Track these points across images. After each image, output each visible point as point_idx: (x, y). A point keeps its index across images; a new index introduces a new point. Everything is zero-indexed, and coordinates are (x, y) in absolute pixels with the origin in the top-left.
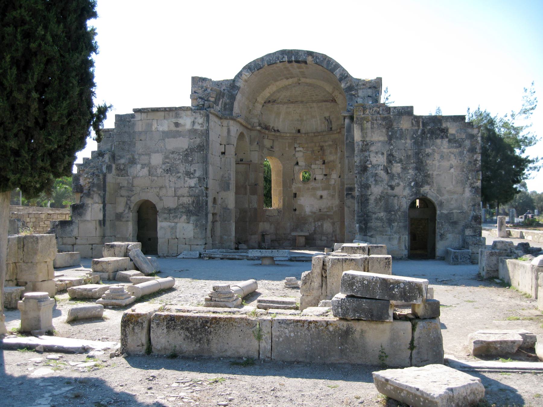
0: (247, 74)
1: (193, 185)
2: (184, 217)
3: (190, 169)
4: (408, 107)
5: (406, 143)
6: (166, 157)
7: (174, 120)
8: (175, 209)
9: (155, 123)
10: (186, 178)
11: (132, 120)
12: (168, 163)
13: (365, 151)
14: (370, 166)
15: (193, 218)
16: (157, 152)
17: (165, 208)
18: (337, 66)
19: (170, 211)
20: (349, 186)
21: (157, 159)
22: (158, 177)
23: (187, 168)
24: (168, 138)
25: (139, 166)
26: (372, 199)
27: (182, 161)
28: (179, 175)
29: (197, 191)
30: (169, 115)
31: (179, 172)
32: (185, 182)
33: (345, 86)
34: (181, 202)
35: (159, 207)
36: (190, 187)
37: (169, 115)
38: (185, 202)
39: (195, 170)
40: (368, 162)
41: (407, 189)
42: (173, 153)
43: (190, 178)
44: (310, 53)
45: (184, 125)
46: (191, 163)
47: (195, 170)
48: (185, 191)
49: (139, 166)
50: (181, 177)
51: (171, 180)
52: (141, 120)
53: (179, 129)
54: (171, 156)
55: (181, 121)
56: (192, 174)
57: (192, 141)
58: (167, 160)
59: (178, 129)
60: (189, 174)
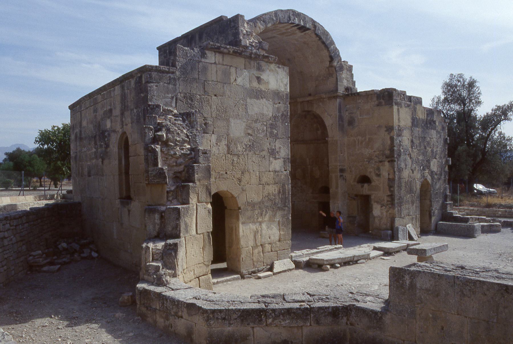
0: (262, 27)
1: (278, 169)
2: (270, 213)
3: (275, 146)
4: (417, 98)
5: (419, 131)
6: (249, 127)
7: (256, 73)
8: (260, 203)
9: (233, 70)
10: (271, 159)
11: (203, 60)
12: (251, 135)
13: (400, 136)
14: (402, 151)
15: (279, 214)
16: (237, 116)
17: (248, 203)
18: (332, 43)
19: (252, 205)
20: (341, 167)
21: (237, 128)
22: (238, 156)
23: (272, 144)
24: (251, 98)
25: (214, 138)
26: (403, 181)
27: (266, 134)
28: (264, 153)
29: (283, 177)
30: (250, 63)
31: (263, 150)
32: (270, 163)
33: (337, 64)
34: (266, 193)
35: (241, 201)
36: (275, 172)
37: (250, 63)
38: (271, 192)
39: (280, 148)
40: (401, 147)
41: (420, 171)
42: (256, 121)
43: (275, 159)
44: (314, 22)
45: (268, 83)
46: (276, 137)
47: (280, 148)
48: (268, 177)
49: (214, 138)
50: (266, 157)
51: (254, 160)
52: (215, 63)
53: (263, 87)
54: (254, 125)
55: (264, 76)
56: (278, 152)
57: (276, 106)
58: (250, 132)
59: (261, 87)
60: (273, 153)
